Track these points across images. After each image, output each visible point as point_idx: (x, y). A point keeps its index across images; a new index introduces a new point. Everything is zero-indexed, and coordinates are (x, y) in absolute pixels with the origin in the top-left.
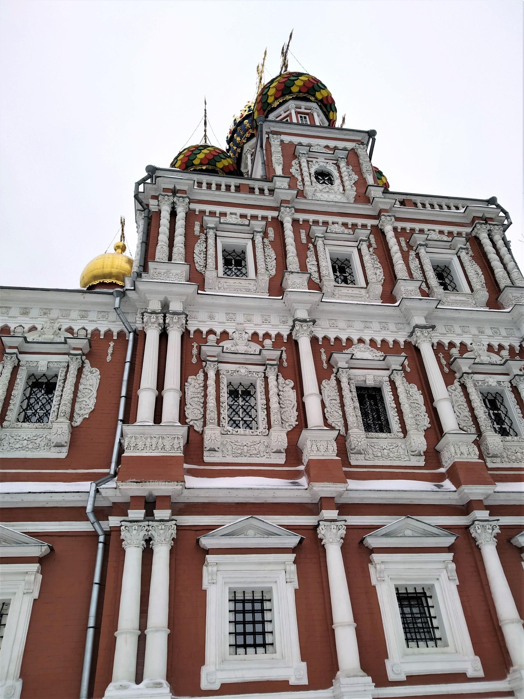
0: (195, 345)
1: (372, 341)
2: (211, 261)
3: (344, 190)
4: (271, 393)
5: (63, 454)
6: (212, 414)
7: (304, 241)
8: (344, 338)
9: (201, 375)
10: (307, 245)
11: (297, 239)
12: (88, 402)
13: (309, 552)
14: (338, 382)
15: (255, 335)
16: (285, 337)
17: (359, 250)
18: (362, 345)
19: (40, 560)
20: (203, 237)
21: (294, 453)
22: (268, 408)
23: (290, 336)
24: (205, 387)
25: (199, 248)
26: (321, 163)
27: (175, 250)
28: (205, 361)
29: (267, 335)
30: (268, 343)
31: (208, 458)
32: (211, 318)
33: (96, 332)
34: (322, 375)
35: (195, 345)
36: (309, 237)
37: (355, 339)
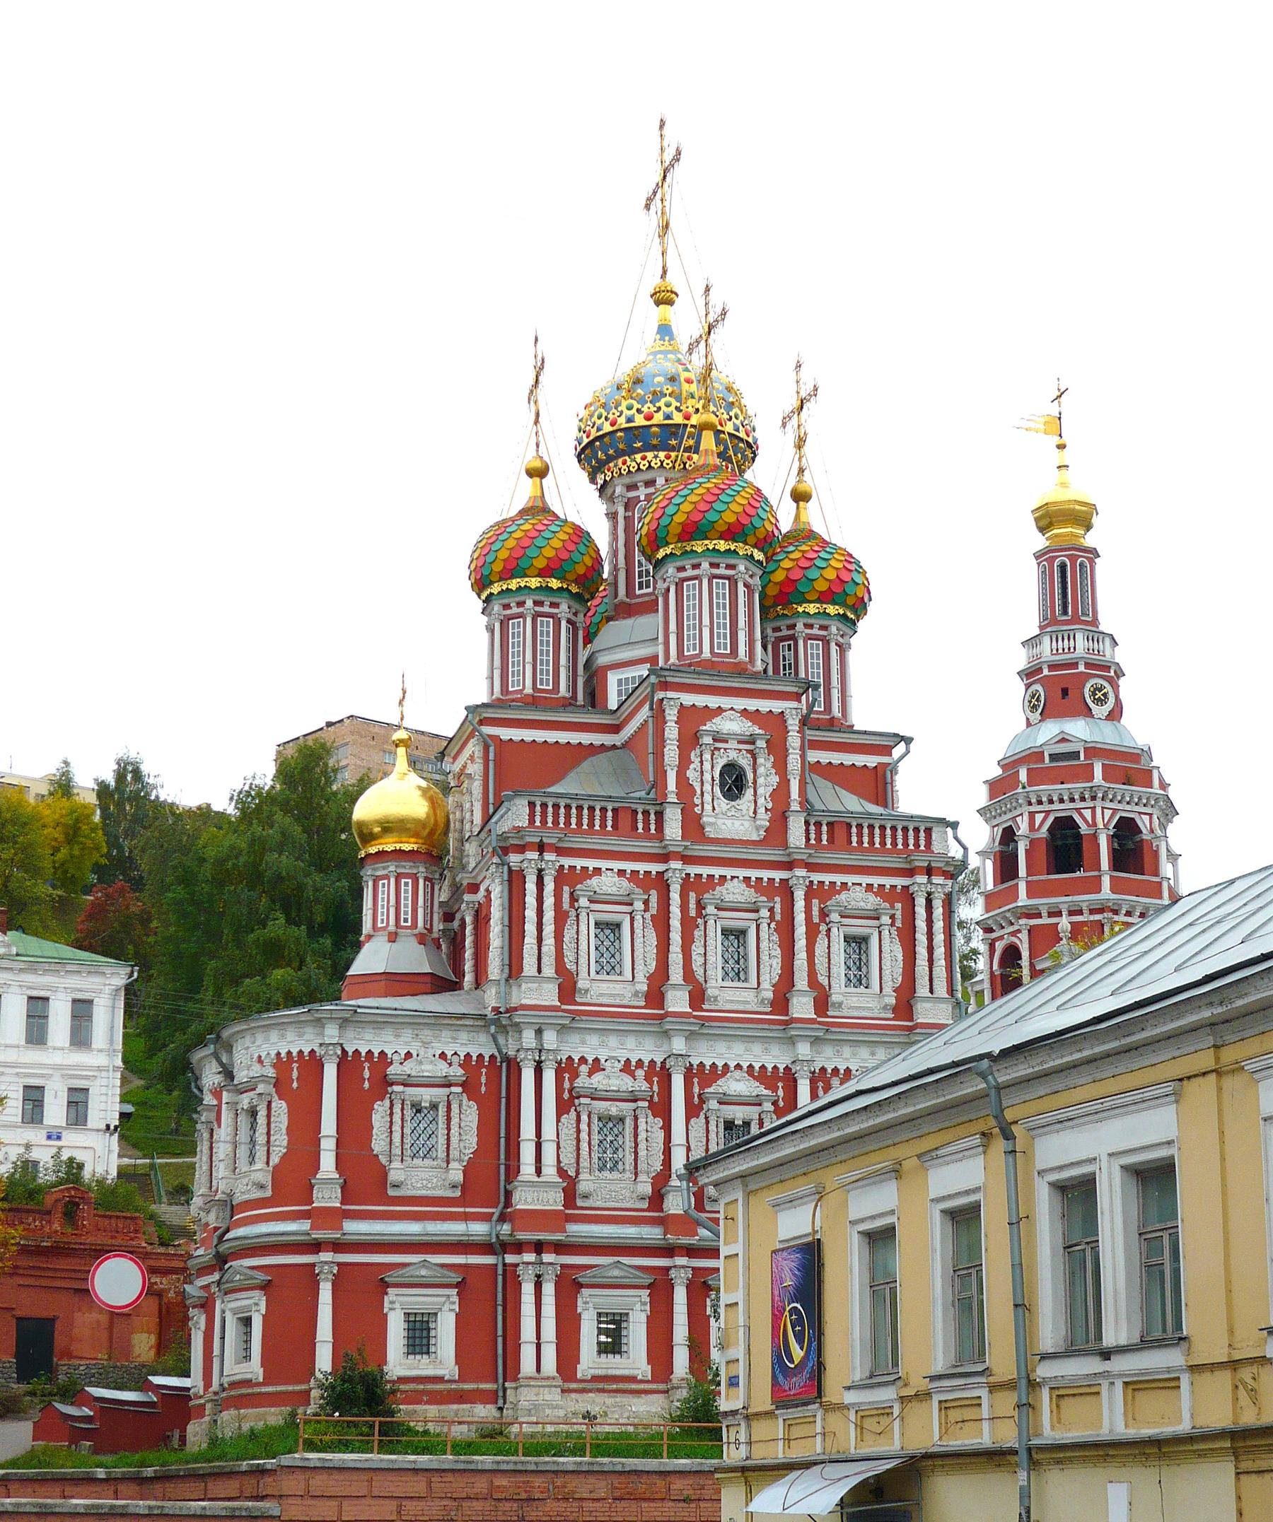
0: (567, 1076)
1: (750, 1066)
2: (583, 961)
3: (755, 812)
4: (640, 1138)
5: (458, 1193)
6: (584, 1163)
7: (693, 913)
8: (720, 1064)
9: (573, 1114)
10: (695, 919)
11: (684, 907)
12: (472, 1141)
13: (660, 1289)
14: (707, 1123)
15: (628, 1061)
16: (659, 1065)
17: (758, 926)
18: (738, 1074)
19: (457, 1285)
20: (573, 913)
21: (657, 1199)
22: (636, 1153)
23: (663, 1063)
24: (578, 1131)
25: (569, 934)
26: (733, 753)
27: (544, 949)
28: (578, 1098)
29: (640, 1063)
30: (640, 1073)
31: (579, 1203)
32: (583, 1042)
33: (468, 1056)
34: (693, 1110)
35: (567, 1076)
36: (700, 907)
37: (732, 1065)
